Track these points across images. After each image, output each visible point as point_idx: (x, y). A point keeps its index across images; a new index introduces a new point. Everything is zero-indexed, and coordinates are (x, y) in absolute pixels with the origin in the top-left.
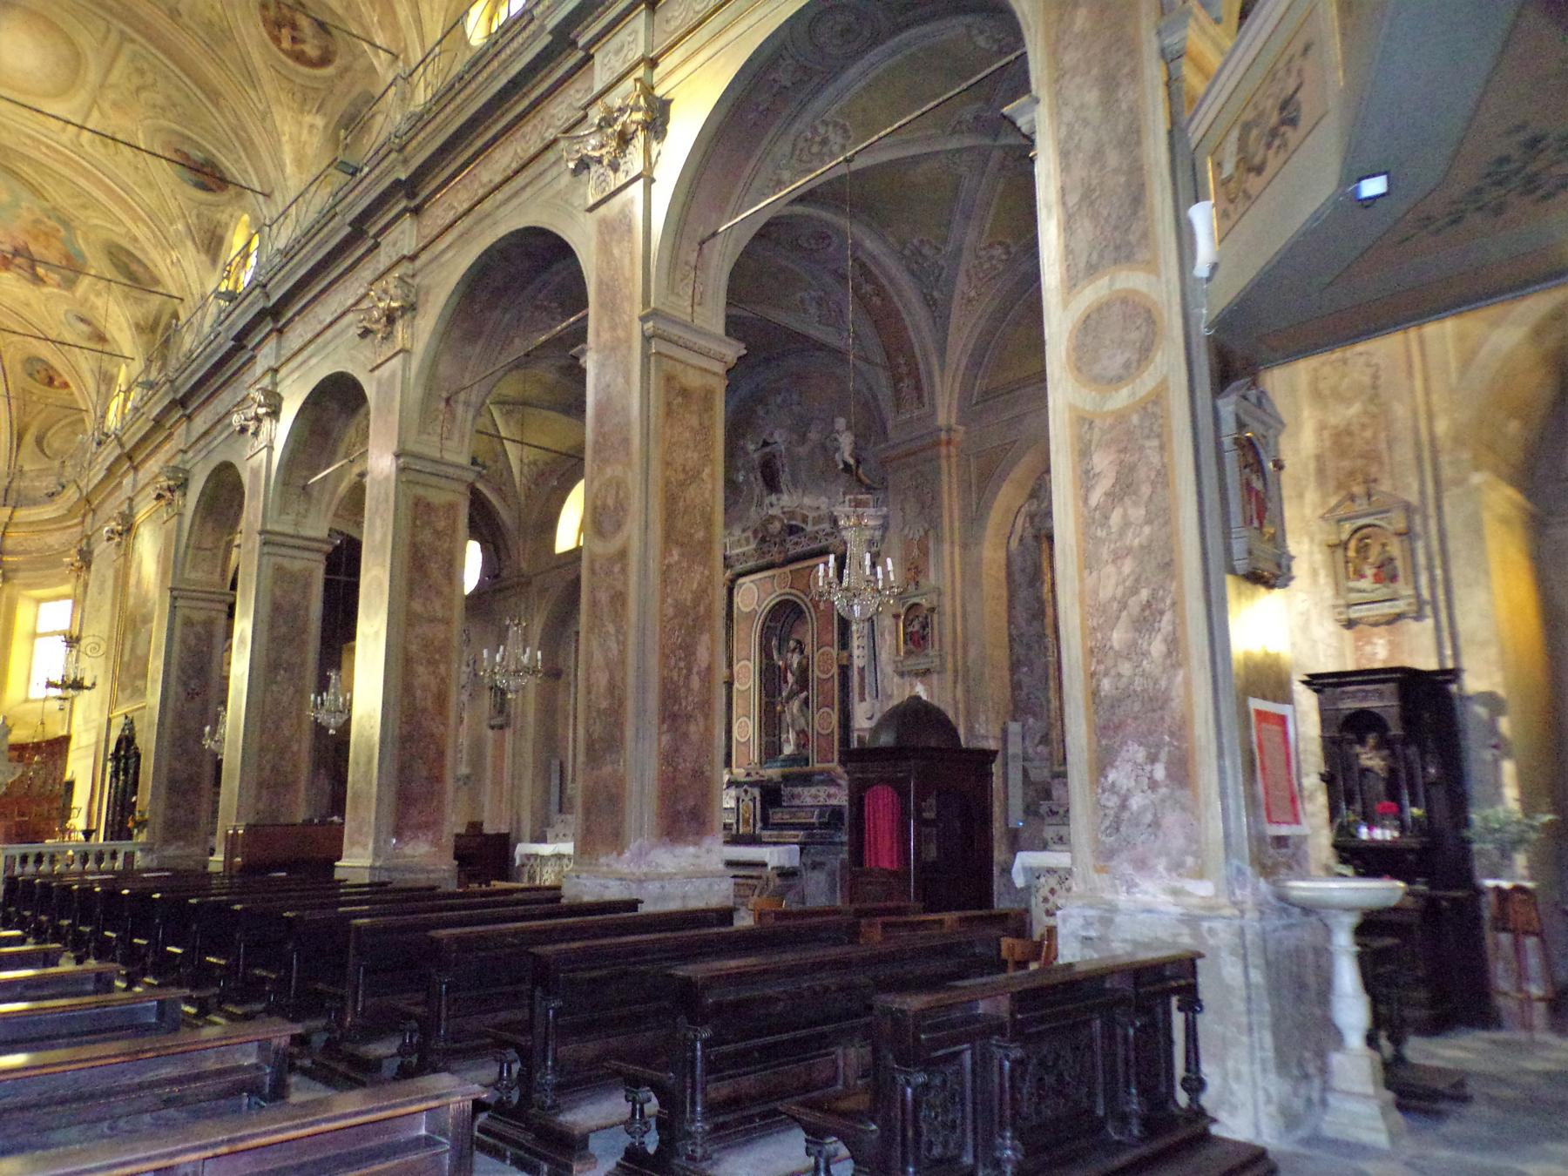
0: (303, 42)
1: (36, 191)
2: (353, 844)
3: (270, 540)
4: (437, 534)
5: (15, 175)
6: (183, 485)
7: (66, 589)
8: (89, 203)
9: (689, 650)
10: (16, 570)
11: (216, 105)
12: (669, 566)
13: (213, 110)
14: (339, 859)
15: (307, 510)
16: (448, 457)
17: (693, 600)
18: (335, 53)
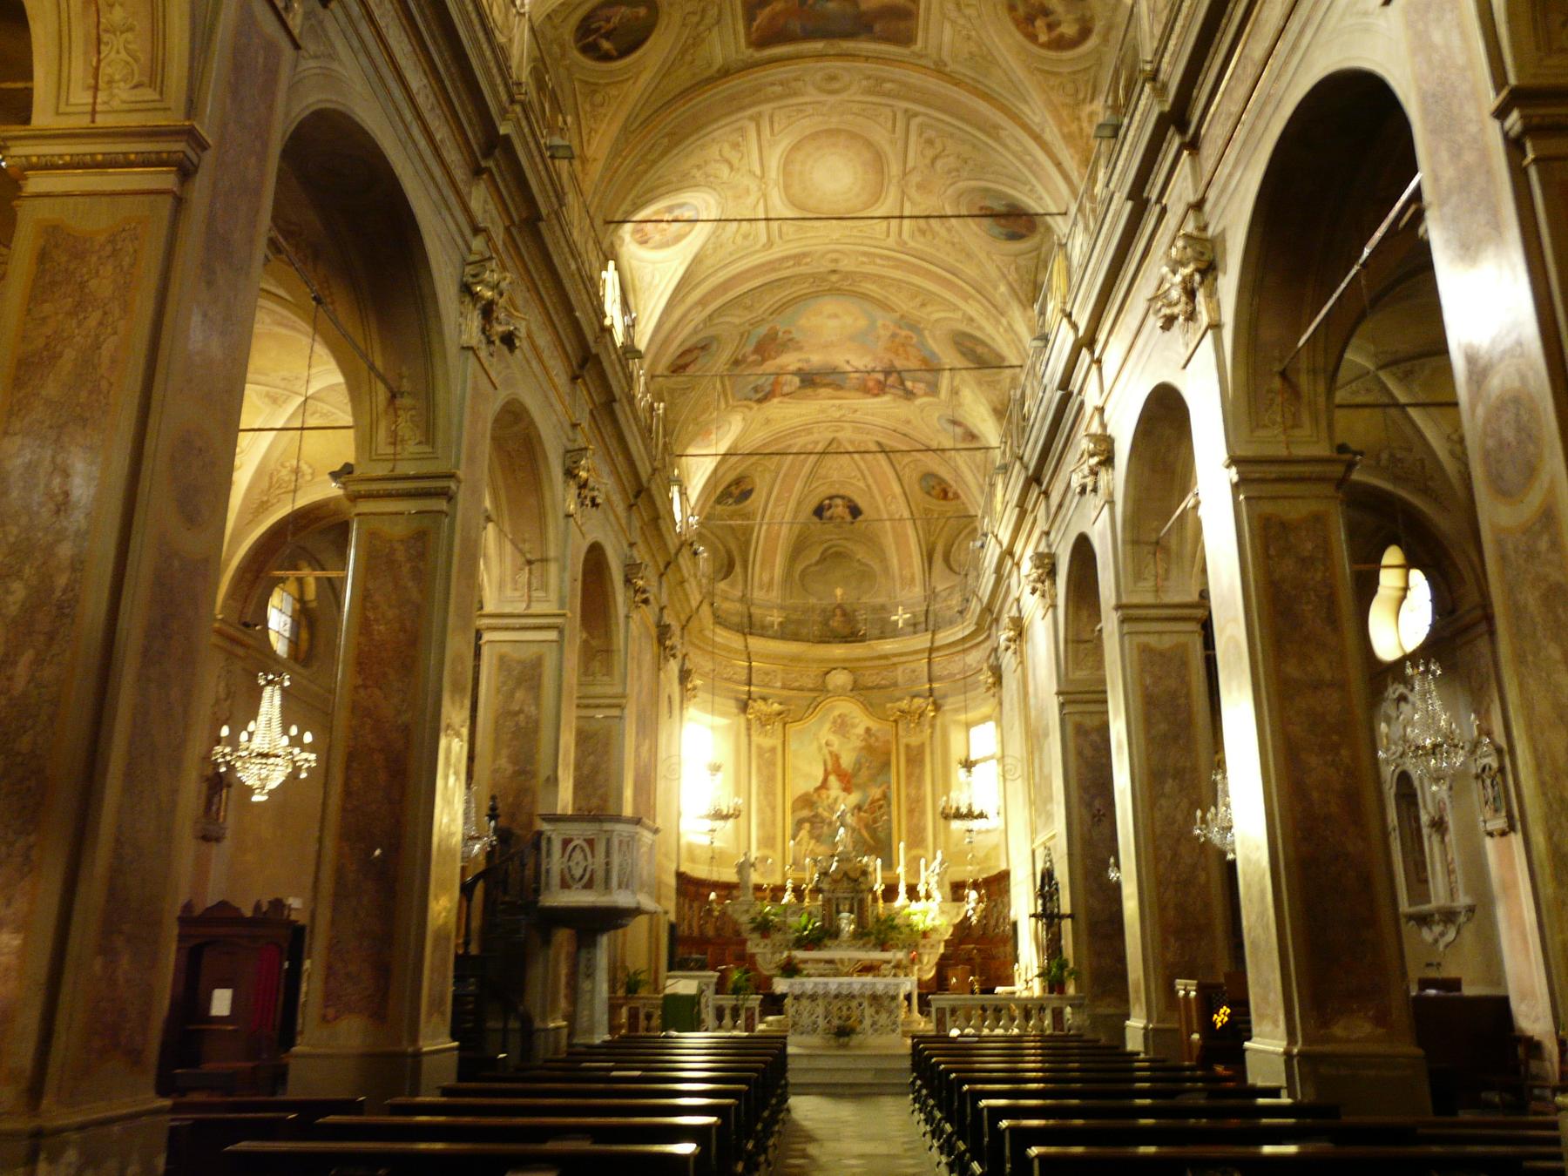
0: (1059, 24)
1: (885, 306)
2: (1261, 1017)
3: (1130, 615)
4: (1305, 562)
5: (865, 297)
6: (1052, 573)
7: (986, 709)
8: (927, 299)
10: (945, 696)
11: (998, 139)
13: (990, 142)
14: (1249, 1039)
15: (1167, 571)
18: (1092, 18)
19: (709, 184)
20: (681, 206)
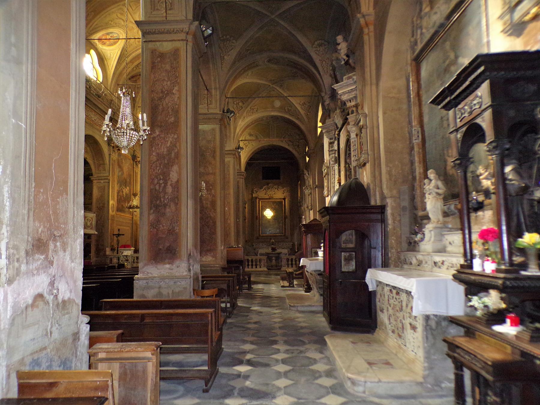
4: (209, 142)
9: (165, 176)
12: (154, 138)
16: (211, 111)
17: (168, 151)
19: (117, 26)
20: (111, 33)
